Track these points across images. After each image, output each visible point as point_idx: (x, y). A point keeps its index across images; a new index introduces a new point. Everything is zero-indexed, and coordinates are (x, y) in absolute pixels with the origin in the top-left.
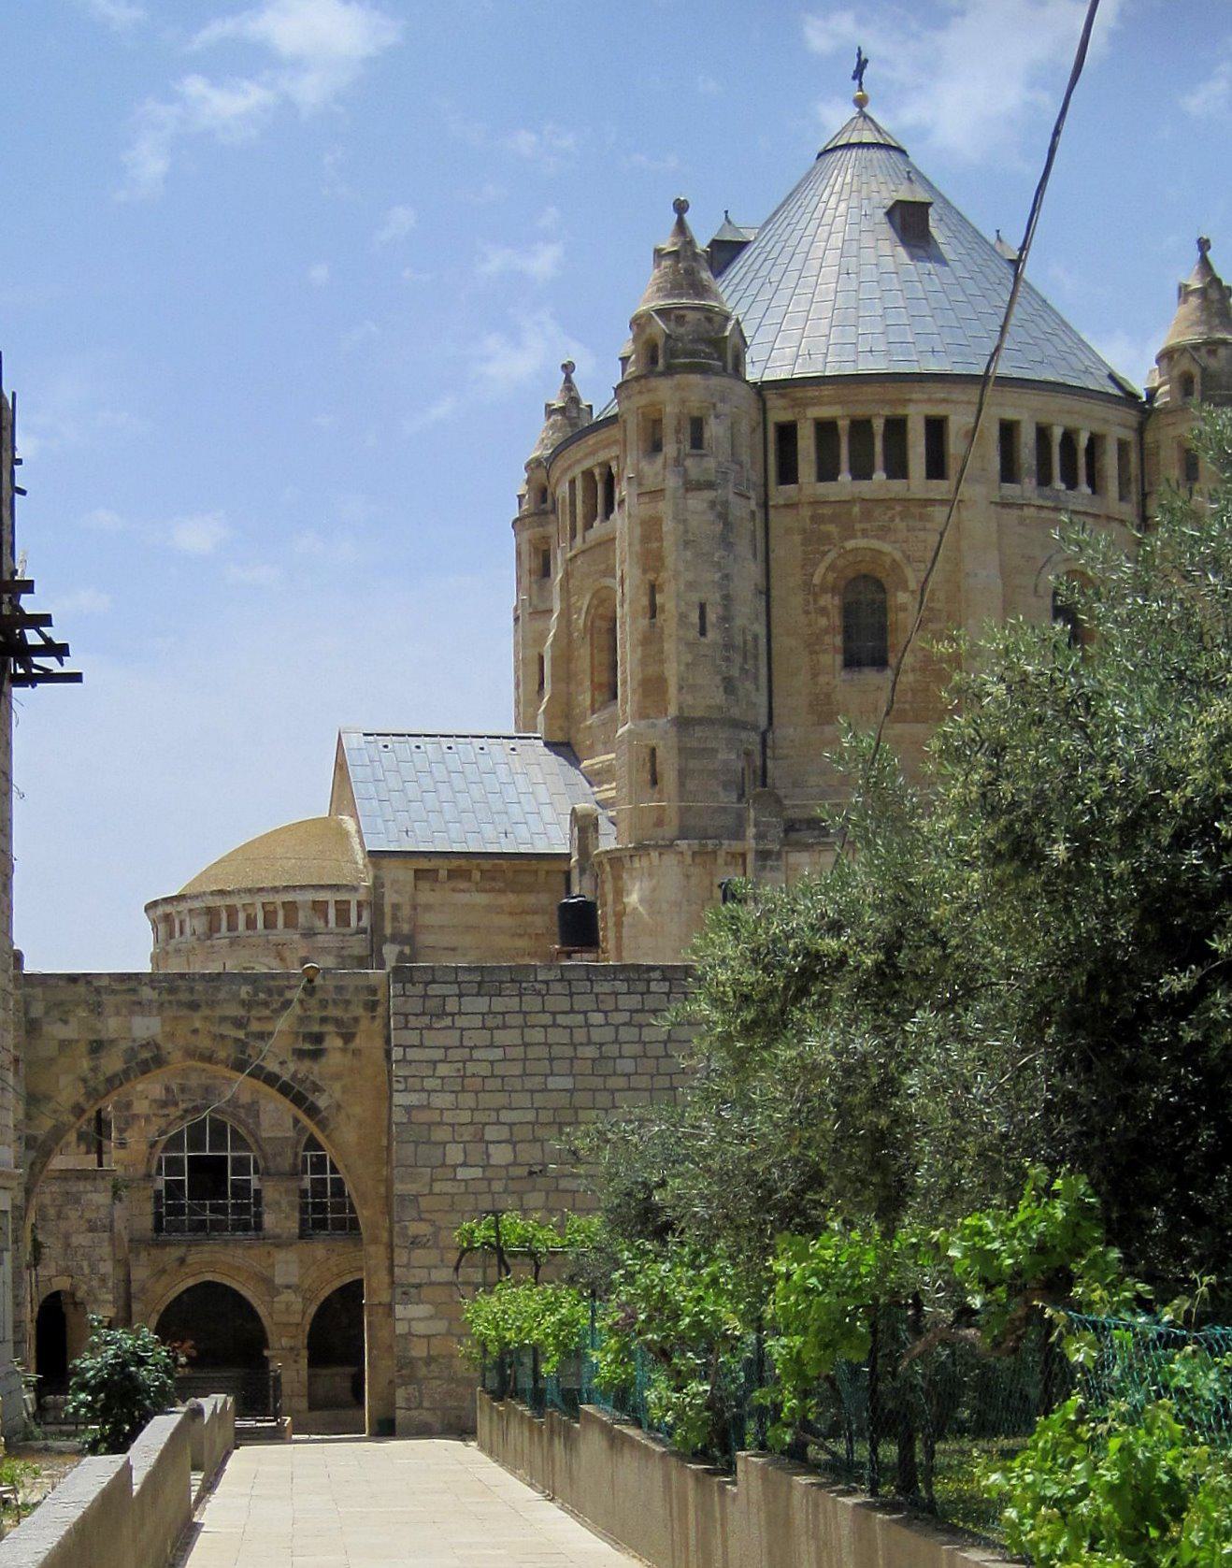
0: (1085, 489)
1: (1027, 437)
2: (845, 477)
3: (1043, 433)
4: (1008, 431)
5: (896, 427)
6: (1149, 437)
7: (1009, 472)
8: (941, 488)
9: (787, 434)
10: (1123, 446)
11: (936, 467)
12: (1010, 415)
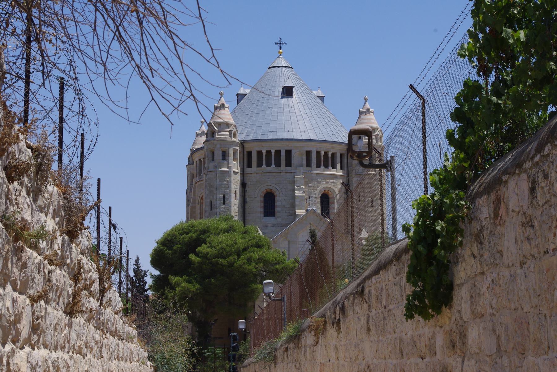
1: (314, 156)
2: (264, 166)
3: (318, 153)
4: (308, 153)
5: (278, 152)
7: (309, 164)
9: (250, 153)
10: (342, 155)
11: (289, 163)
12: (309, 149)
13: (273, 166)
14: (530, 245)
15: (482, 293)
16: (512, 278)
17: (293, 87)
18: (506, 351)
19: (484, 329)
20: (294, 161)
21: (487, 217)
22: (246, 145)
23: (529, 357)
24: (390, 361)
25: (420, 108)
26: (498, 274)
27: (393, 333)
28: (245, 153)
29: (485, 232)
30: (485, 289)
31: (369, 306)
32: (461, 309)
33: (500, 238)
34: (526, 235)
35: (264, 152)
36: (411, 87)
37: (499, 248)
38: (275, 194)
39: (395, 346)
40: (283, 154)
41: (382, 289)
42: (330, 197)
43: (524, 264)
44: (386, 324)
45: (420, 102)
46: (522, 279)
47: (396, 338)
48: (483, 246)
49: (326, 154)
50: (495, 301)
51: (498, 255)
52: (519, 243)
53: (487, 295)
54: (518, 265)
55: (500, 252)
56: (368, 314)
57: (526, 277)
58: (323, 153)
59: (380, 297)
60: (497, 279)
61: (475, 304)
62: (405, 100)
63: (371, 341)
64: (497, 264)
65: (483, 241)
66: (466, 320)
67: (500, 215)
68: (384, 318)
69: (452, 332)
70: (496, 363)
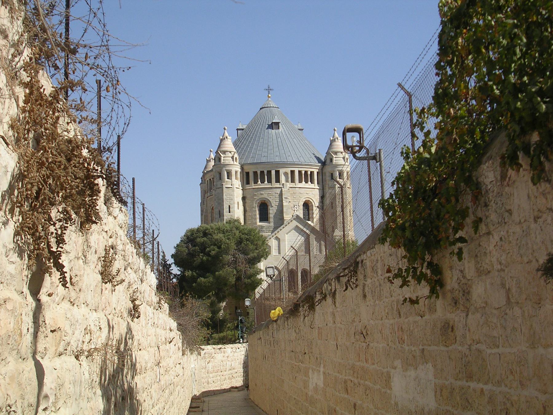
0: (309, 183)
3: (300, 172)
4: (293, 172)
6: (325, 171)
8: (277, 185)
9: (248, 174)
11: (278, 180)
13: (266, 182)
14: (547, 199)
15: (488, 251)
16: (525, 233)
17: (279, 122)
18: (518, 303)
19: (492, 284)
20: (283, 178)
21: (493, 181)
22: (245, 167)
23: (547, 305)
24: (387, 321)
25: (408, 103)
26: (507, 232)
27: (390, 296)
28: (244, 173)
29: (491, 194)
30: (492, 247)
31: (365, 276)
32: (464, 269)
33: (508, 198)
34: (541, 190)
35: (259, 172)
36: (400, 85)
37: (508, 208)
38: (268, 204)
39: (392, 308)
40: (273, 173)
41: (377, 260)
42: (310, 205)
43: (538, 218)
44: (383, 290)
45: (407, 98)
46: (537, 233)
47: (393, 301)
48: (489, 208)
49: (306, 172)
50: (504, 257)
51: (507, 214)
52: (533, 199)
53: (494, 252)
54: (532, 220)
55: (510, 212)
56: (364, 283)
57: (542, 230)
58: (303, 172)
59: (375, 268)
60: (506, 236)
61: (480, 262)
62: (394, 97)
63: (368, 306)
64: (505, 223)
65: (488, 203)
66: (470, 278)
67: (509, 176)
68: (380, 285)
69: (455, 290)
70: (506, 314)
